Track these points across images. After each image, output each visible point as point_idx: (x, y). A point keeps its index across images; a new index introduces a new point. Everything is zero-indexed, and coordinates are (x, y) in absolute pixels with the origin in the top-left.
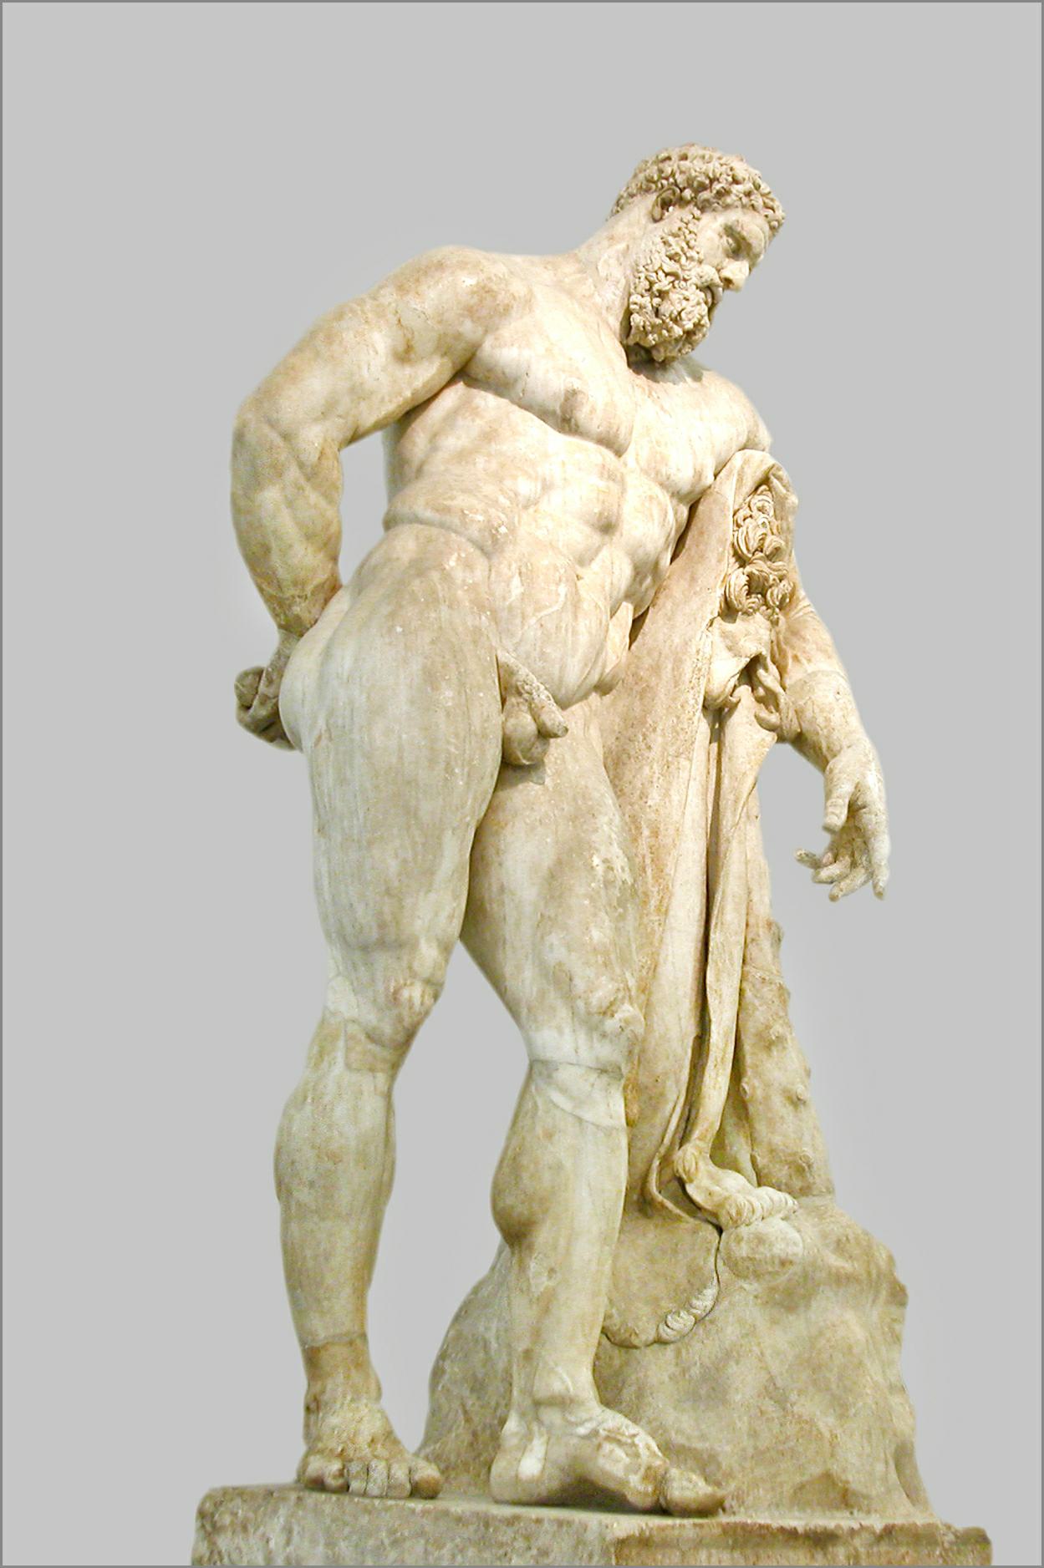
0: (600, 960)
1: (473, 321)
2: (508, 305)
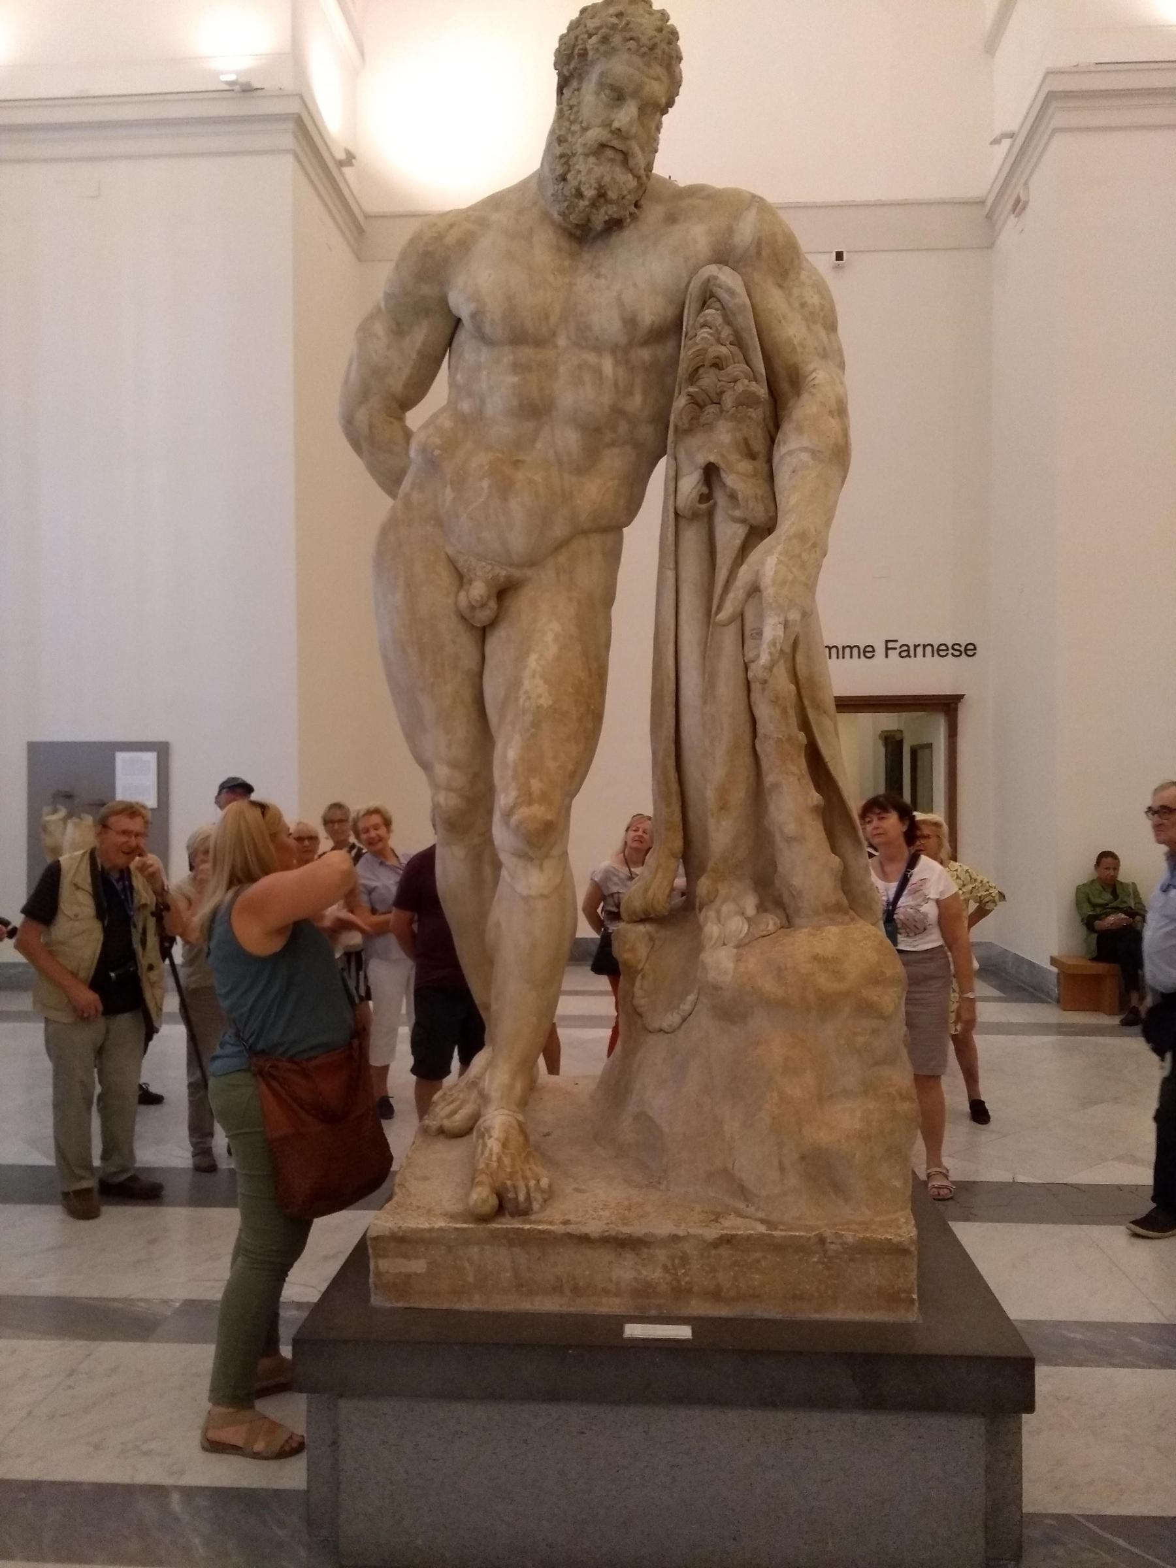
0: (510, 773)
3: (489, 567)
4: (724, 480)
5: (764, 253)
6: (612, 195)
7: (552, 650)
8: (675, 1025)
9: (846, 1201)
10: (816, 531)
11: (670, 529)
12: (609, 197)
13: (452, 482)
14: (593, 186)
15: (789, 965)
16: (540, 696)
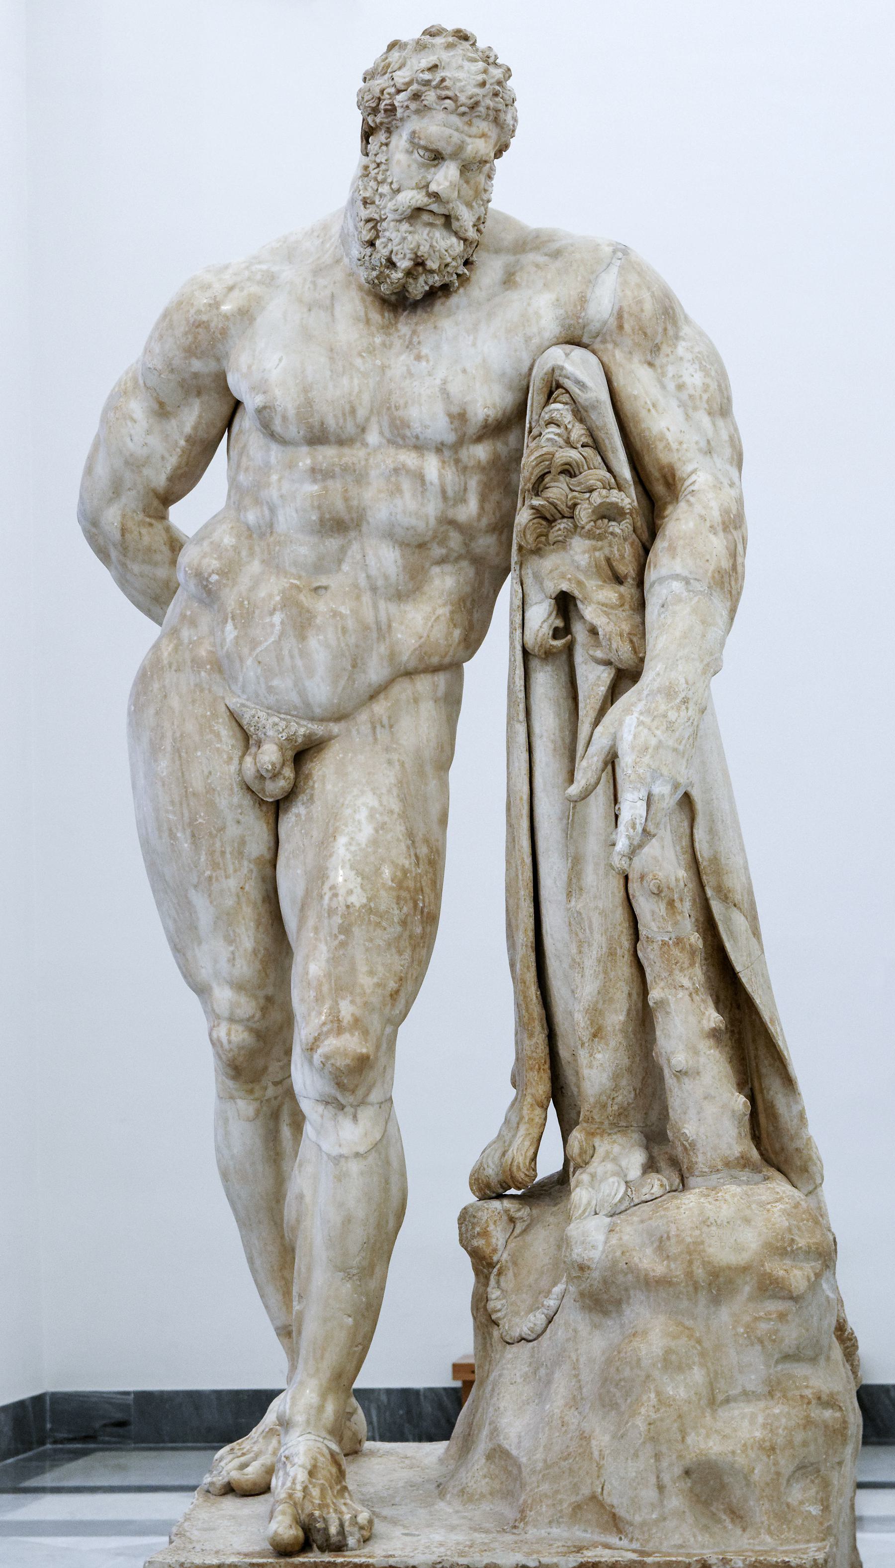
0: (312, 994)
1: (197, 358)
2: (223, 328)
3: (283, 724)
4: (582, 612)
5: (627, 327)
6: (432, 265)
7: (366, 832)
8: (539, 1329)
9: (744, 1530)
10: (687, 683)
11: (517, 672)
12: (428, 267)
13: (233, 619)
14: (408, 256)
15: (673, 1233)
16: (350, 892)
